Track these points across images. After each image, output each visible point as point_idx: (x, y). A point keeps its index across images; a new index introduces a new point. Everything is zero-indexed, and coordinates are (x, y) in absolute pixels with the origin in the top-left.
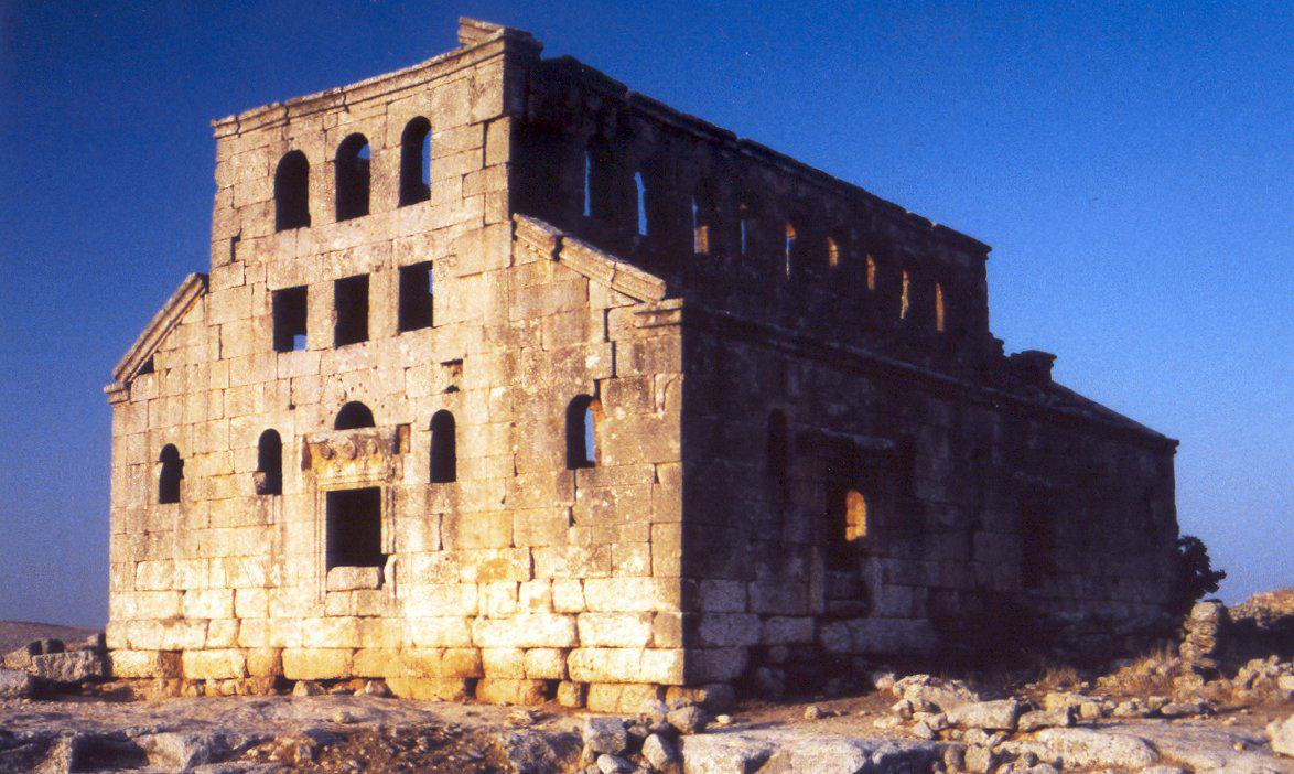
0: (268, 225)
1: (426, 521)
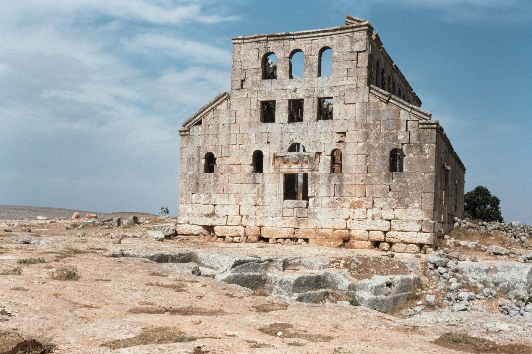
0: (259, 77)
1: (328, 186)
